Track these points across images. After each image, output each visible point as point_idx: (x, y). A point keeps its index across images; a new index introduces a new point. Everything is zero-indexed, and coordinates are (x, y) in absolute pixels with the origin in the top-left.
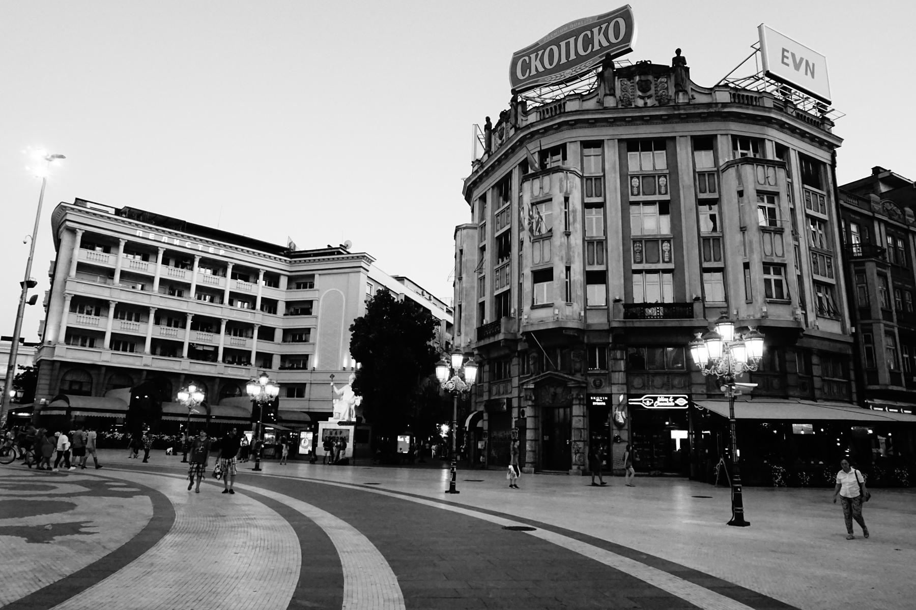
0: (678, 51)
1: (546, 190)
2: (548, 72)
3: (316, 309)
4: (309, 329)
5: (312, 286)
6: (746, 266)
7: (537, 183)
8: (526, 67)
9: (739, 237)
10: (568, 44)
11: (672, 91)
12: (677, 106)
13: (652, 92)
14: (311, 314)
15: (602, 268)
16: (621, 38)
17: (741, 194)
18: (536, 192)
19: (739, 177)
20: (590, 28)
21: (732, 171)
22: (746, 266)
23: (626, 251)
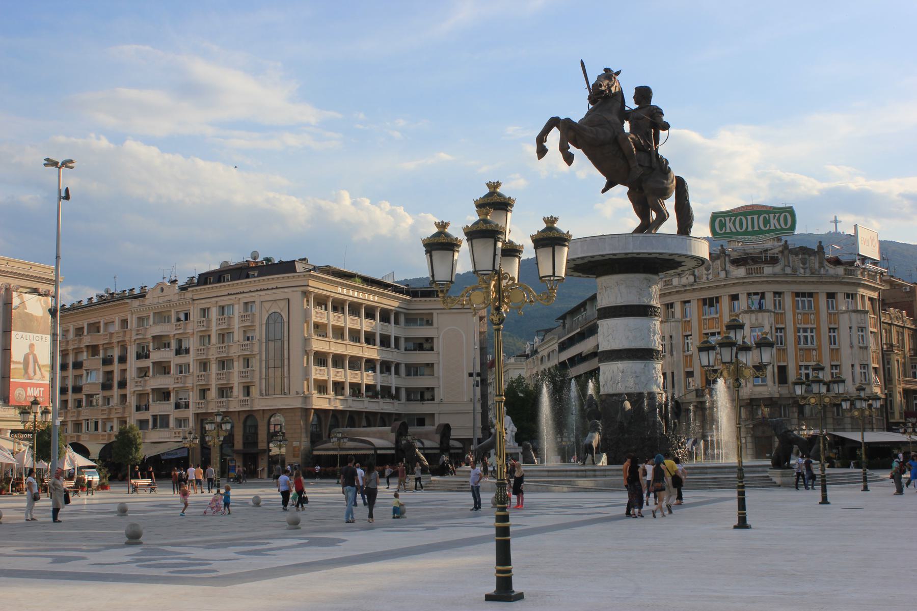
0: (820, 242)
1: (760, 321)
2: (738, 233)
3: (439, 345)
4: (433, 364)
5: (432, 324)
6: (853, 365)
7: (753, 316)
8: (723, 225)
9: (849, 351)
10: (752, 219)
11: (817, 266)
12: (821, 276)
13: (807, 265)
14: (432, 349)
15: (785, 364)
16: (789, 226)
17: (850, 328)
18: (754, 321)
19: (850, 319)
20: (768, 213)
21: (846, 316)
22: (853, 365)
23: (796, 355)
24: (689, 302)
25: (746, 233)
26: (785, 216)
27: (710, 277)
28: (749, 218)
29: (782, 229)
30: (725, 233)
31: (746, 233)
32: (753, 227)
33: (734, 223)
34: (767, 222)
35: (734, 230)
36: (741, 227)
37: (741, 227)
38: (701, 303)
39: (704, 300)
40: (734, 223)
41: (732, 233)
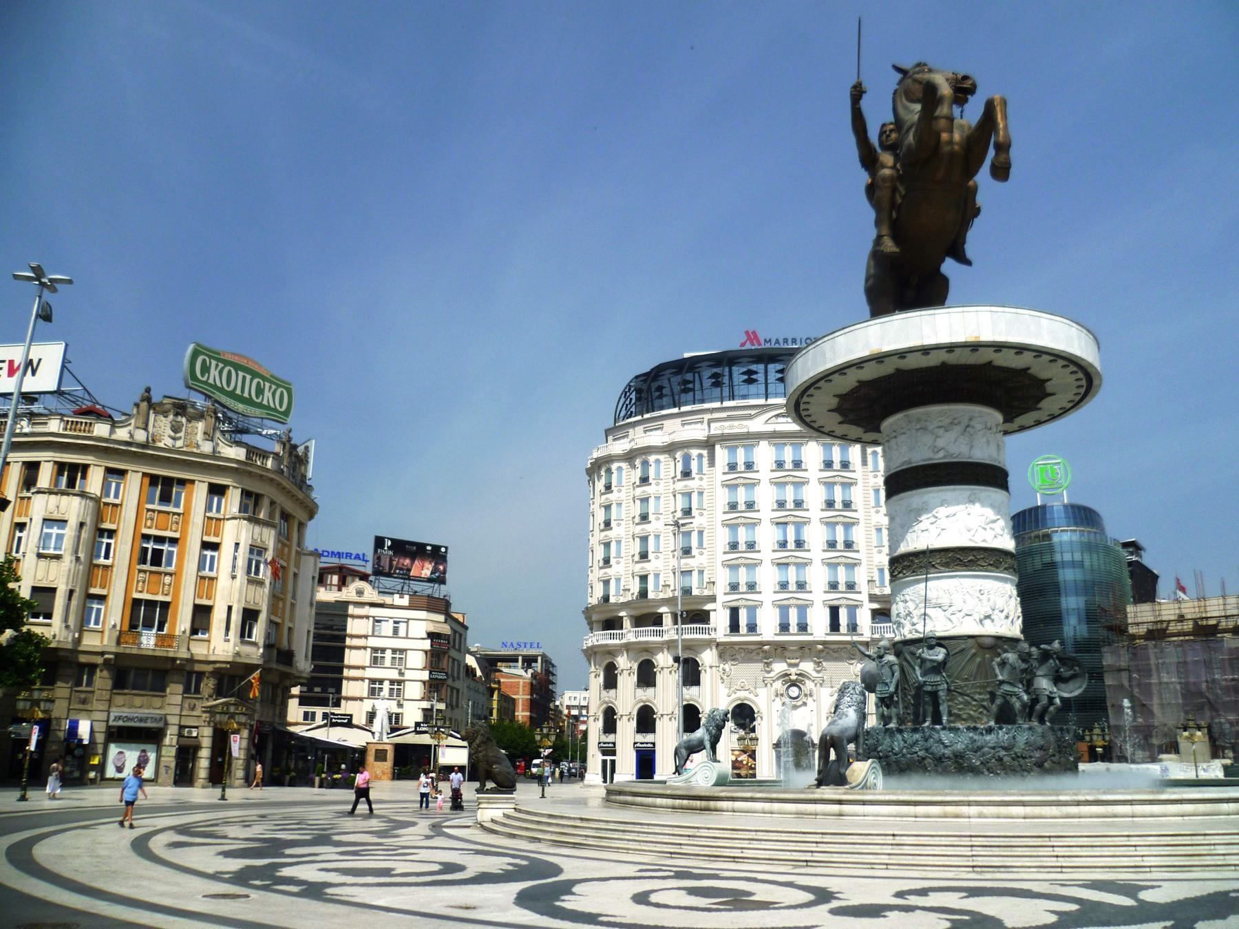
2: (221, 390)
8: (205, 369)
10: (244, 378)
24: (122, 473)
25: (232, 395)
26: (282, 393)
27: (179, 444)
28: (241, 374)
29: (275, 410)
30: (206, 383)
31: (232, 395)
32: (243, 391)
33: (221, 373)
34: (260, 391)
35: (219, 384)
36: (228, 384)
37: (228, 385)
38: (147, 481)
39: (154, 480)
40: (221, 373)
41: (215, 386)
